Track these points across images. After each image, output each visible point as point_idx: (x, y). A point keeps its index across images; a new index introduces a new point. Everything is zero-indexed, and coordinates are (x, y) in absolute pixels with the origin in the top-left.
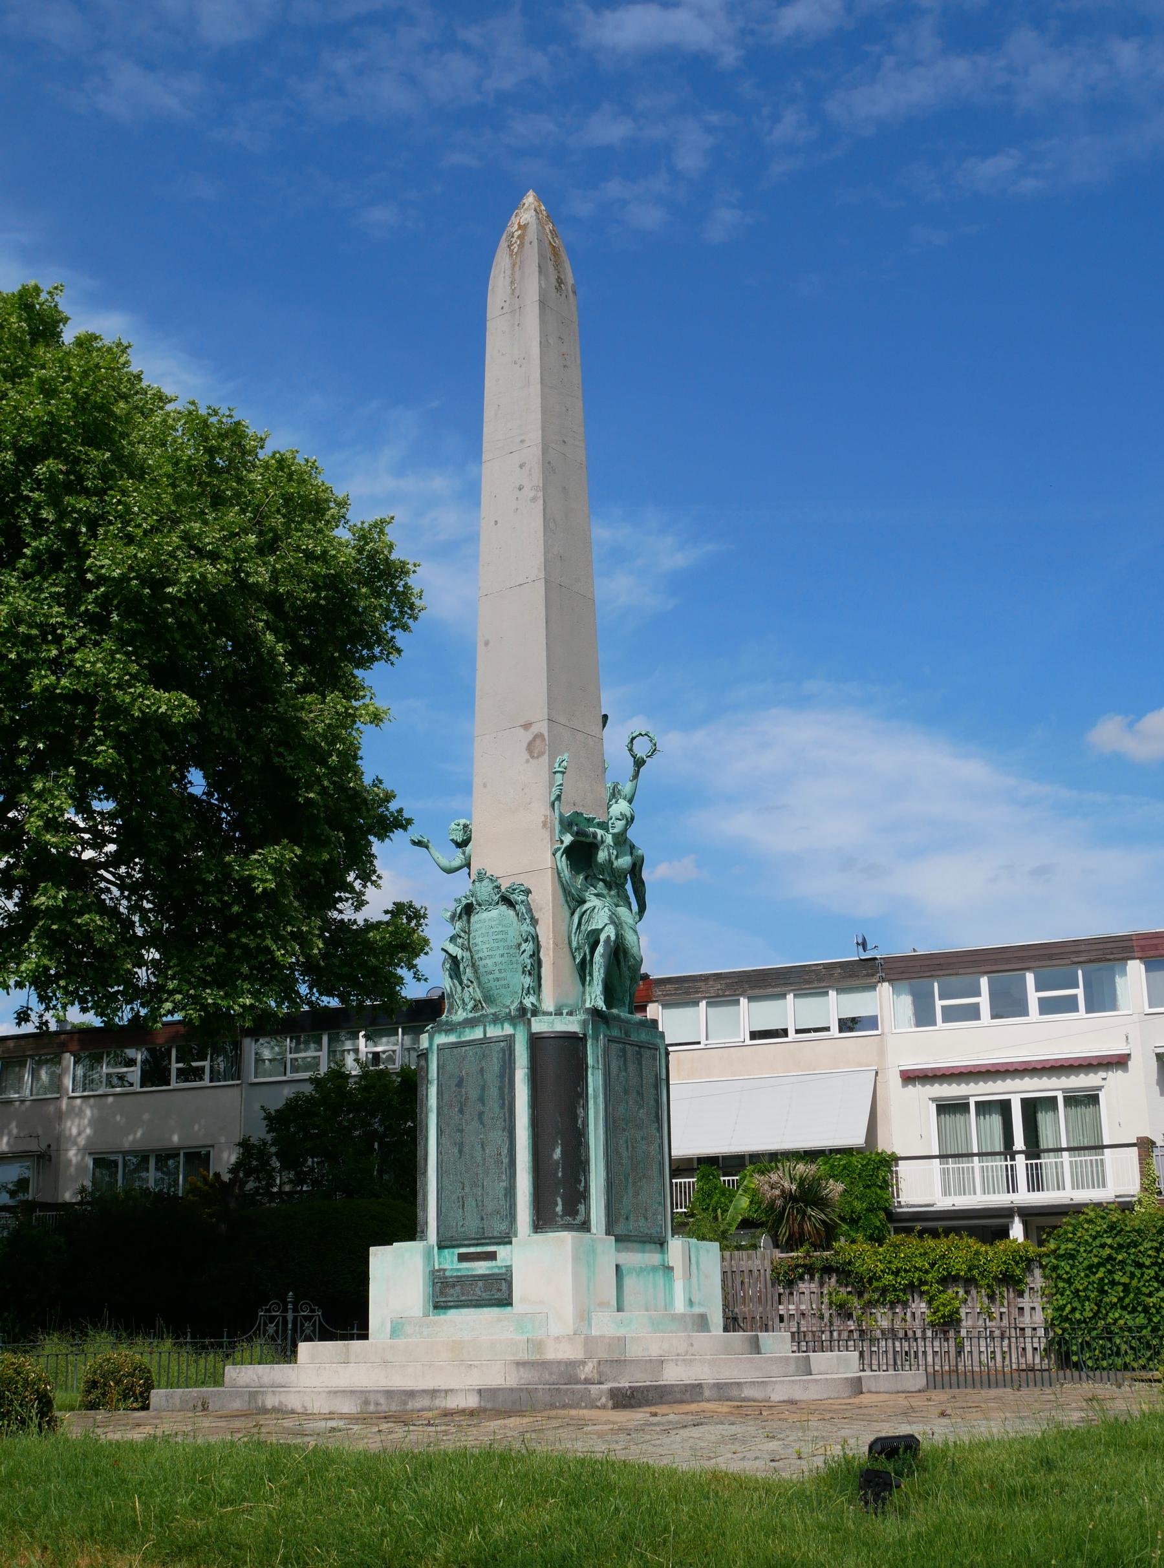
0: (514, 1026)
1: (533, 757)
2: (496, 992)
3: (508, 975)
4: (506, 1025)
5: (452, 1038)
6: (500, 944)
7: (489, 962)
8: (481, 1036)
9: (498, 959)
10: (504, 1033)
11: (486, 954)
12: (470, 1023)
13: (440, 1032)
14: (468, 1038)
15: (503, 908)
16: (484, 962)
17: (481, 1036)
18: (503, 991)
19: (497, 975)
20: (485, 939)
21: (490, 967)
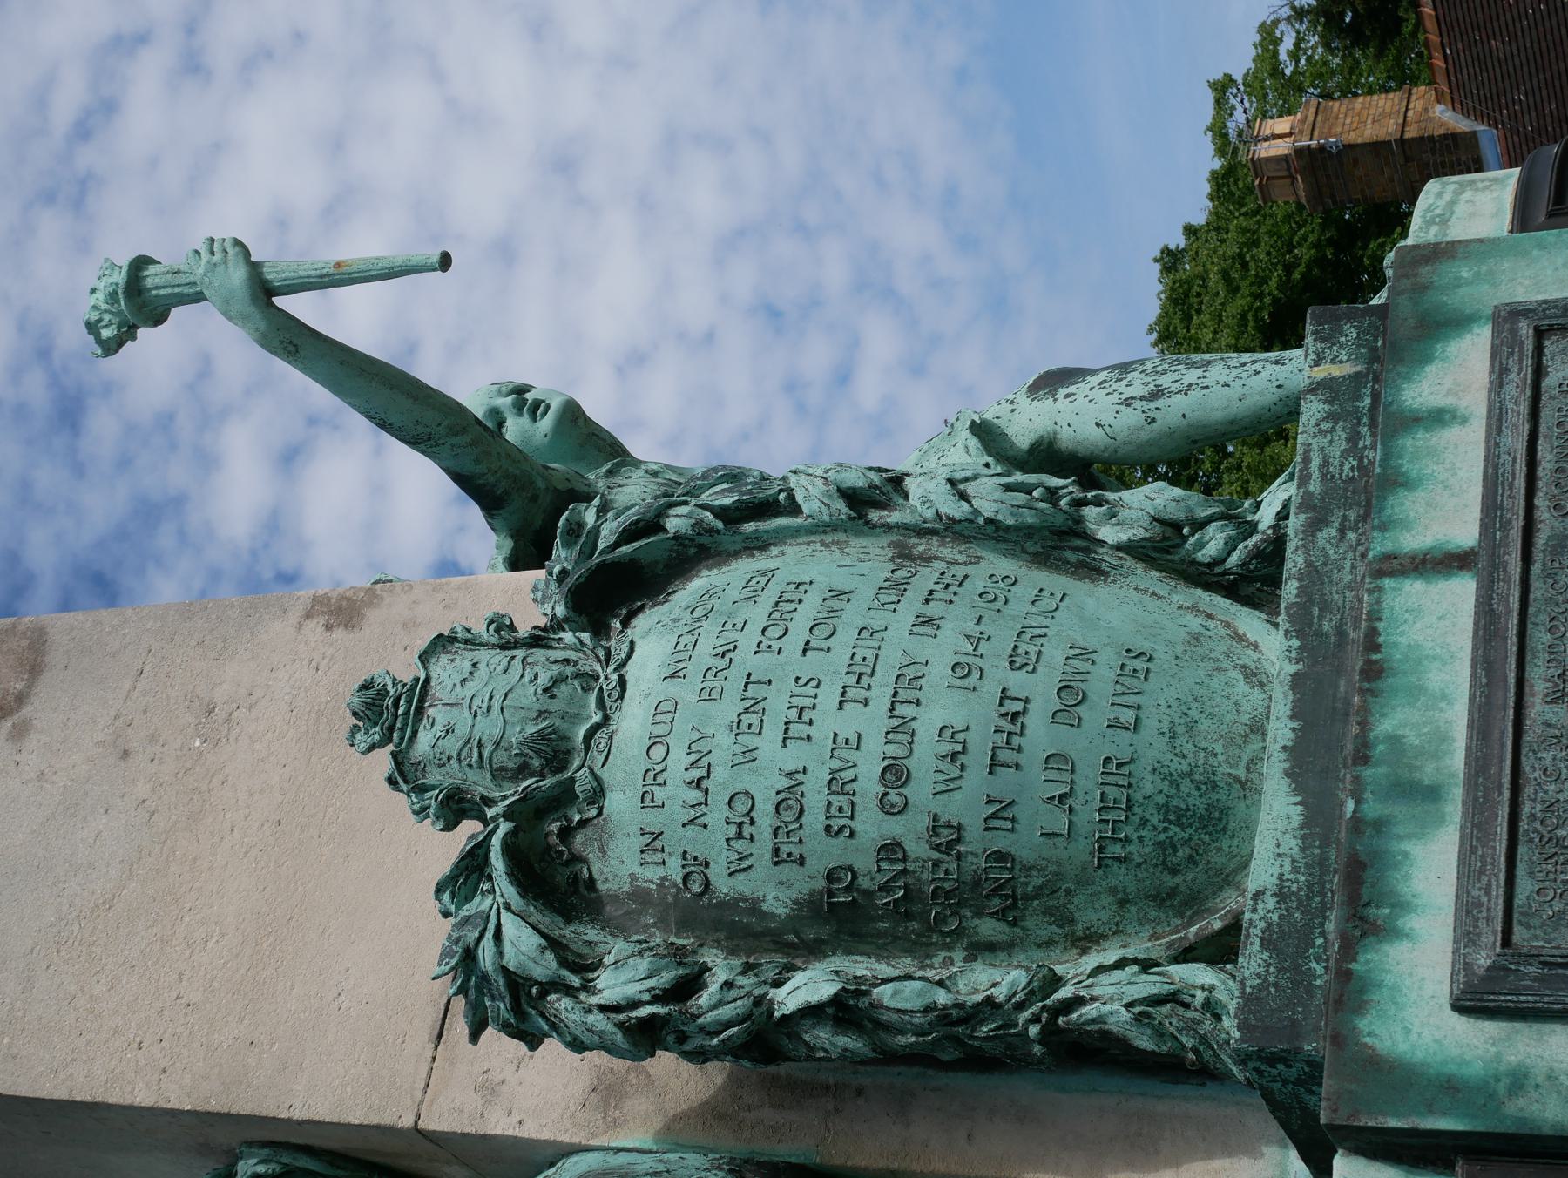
0: (1441, 324)
1: (21, 699)
2: (1151, 747)
3: (1063, 632)
4: (1423, 390)
5: (1430, 870)
6: (852, 616)
7: (937, 711)
8: (1462, 591)
9: (940, 652)
10: (1476, 403)
11: (870, 721)
12: (1345, 672)
13: (1350, 992)
14: (1457, 718)
15: (651, 638)
16: (925, 759)
17: (1462, 591)
18: (1160, 695)
19: (1040, 689)
20: (778, 706)
21: (973, 713)
